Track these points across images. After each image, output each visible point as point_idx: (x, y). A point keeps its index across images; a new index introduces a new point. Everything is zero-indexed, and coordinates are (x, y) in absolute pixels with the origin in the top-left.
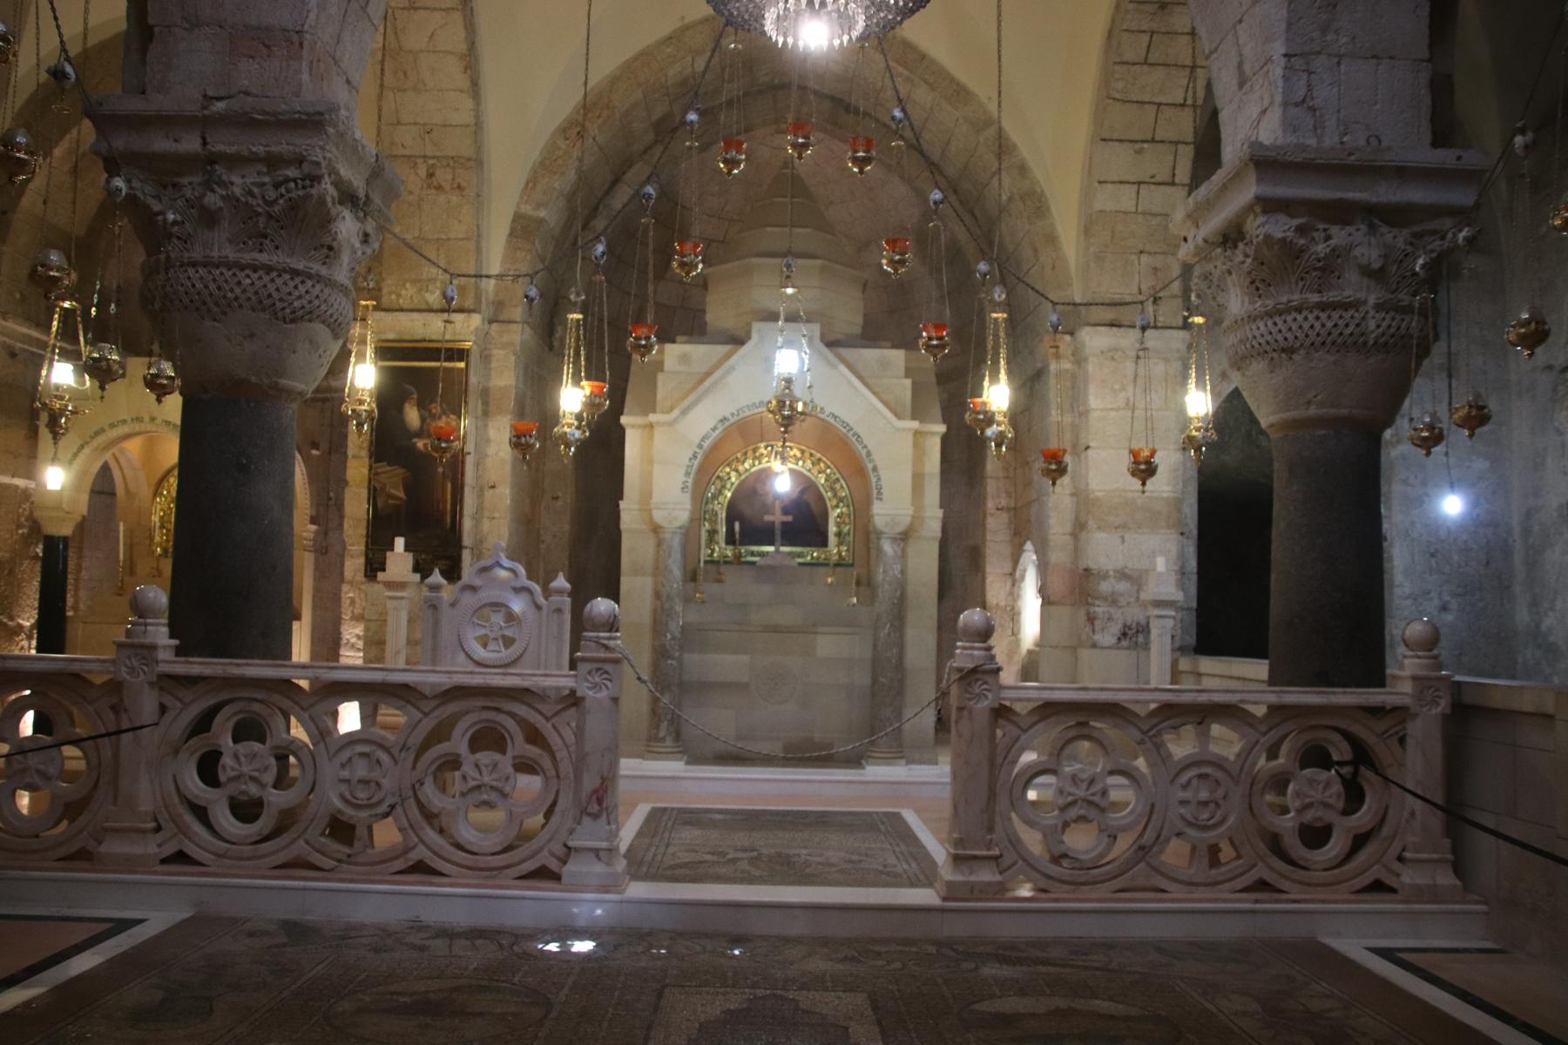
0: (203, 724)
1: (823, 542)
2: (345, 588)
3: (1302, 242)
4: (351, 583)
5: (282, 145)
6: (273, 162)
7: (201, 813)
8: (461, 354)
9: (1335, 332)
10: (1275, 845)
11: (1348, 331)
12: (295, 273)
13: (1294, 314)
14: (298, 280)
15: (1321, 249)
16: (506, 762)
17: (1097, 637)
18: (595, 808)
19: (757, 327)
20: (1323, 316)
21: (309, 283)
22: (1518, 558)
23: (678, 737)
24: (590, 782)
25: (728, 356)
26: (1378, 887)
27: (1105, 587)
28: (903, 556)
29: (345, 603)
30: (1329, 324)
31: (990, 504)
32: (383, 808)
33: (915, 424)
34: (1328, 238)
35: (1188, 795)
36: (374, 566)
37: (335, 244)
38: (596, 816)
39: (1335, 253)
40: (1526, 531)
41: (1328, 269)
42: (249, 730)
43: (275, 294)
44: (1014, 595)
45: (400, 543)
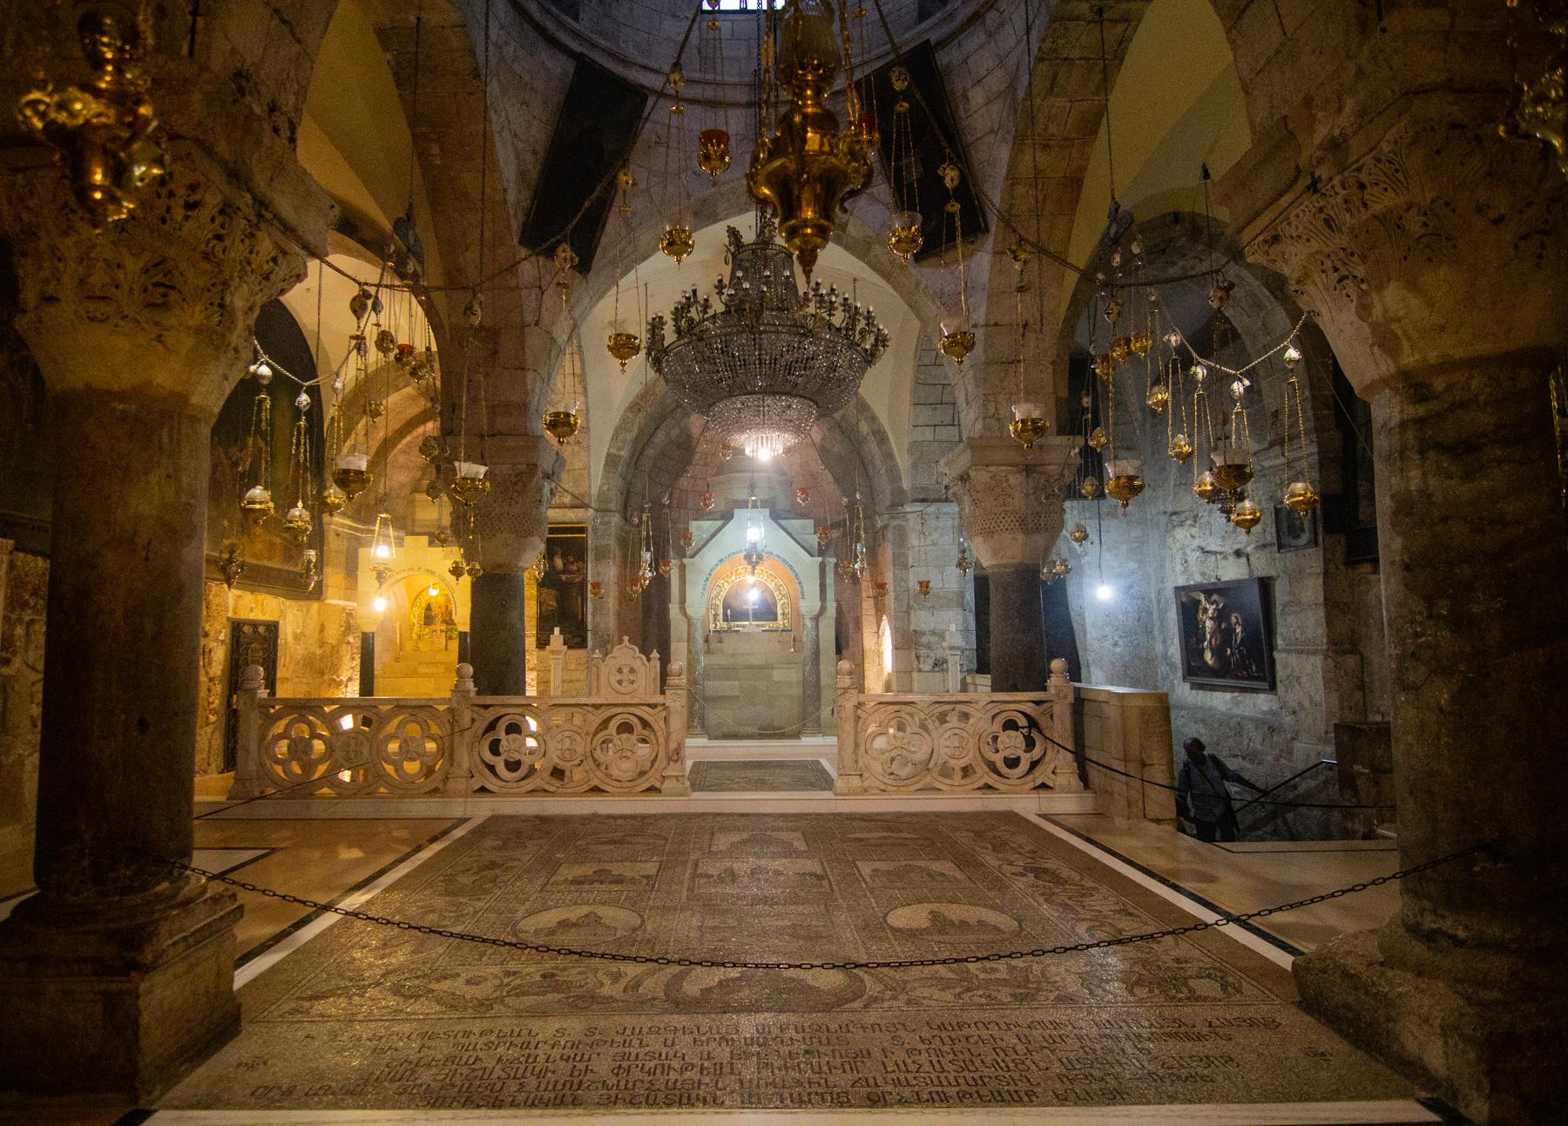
0: (492, 727)
1: (776, 619)
7: (492, 768)
8: (582, 530)
10: (992, 767)
16: (634, 738)
17: (921, 666)
18: (675, 757)
19: (736, 512)
22: (1155, 616)
23: (703, 726)
24: (673, 746)
25: (723, 526)
26: (1044, 786)
27: (924, 640)
31: (864, 595)
32: (577, 762)
33: (820, 559)
35: (948, 743)
36: (542, 643)
38: (676, 761)
40: (1159, 602)
44: (879, 644)
45: (557, 630)
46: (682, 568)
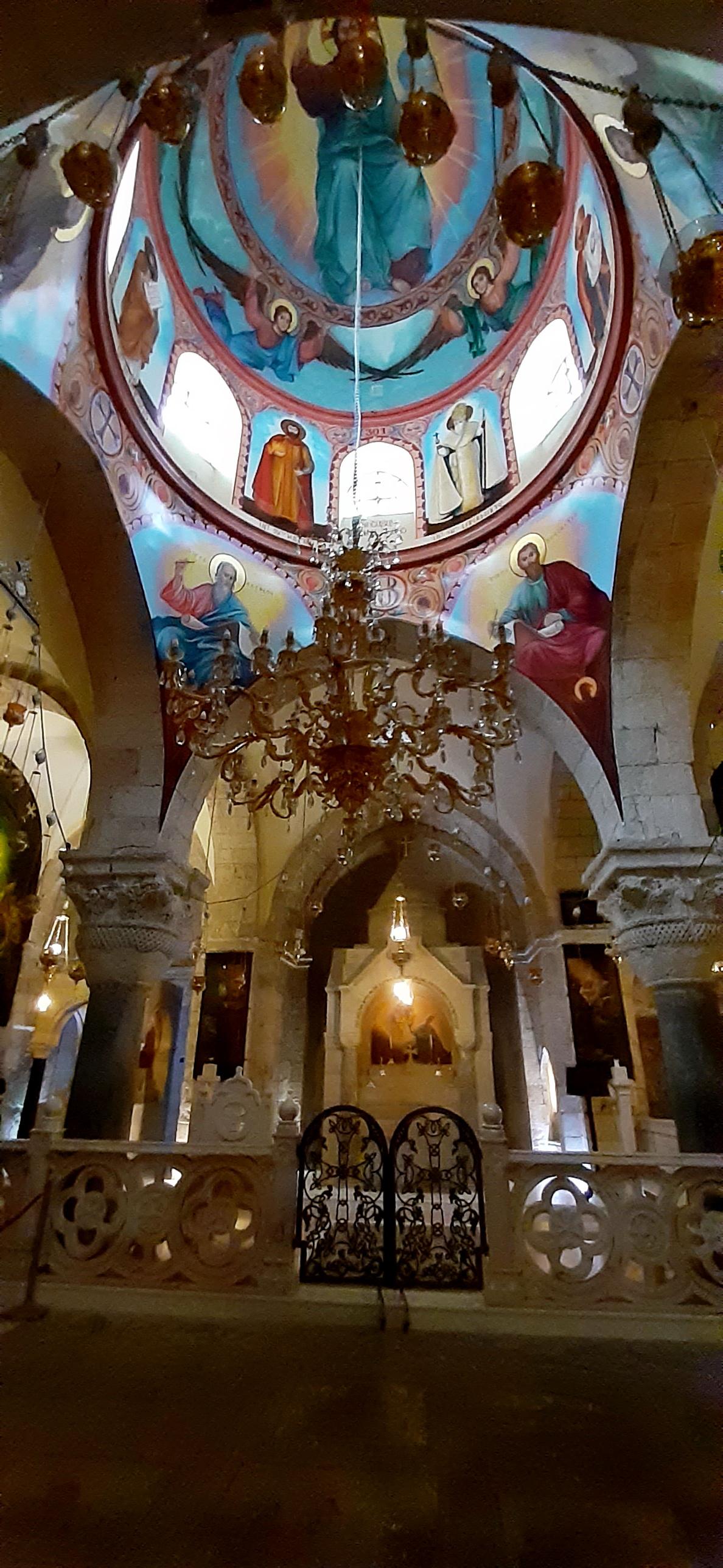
0: (69, 1181)
2: (184, 1084)
3: (646, 889)
4: (187, 1081)
5: (145, 869)
6: (141, 877)
9: (674, 936)
11: (681, 935)
12: (148, 929)
13: (650, 927)
14: (149, 932)
15: (657, 892)
20: (666, 927)
21: (155, 932)
28: (472, 1059)
29: (183, 1091)
30: (670, 932)
34: (660, 886)
36: (198, 1071)
37: (170, 914)
39: (667, 893)
41: (663, 901)
42: (94, 1184)
43: (137, 939)
46: (338, 994)
